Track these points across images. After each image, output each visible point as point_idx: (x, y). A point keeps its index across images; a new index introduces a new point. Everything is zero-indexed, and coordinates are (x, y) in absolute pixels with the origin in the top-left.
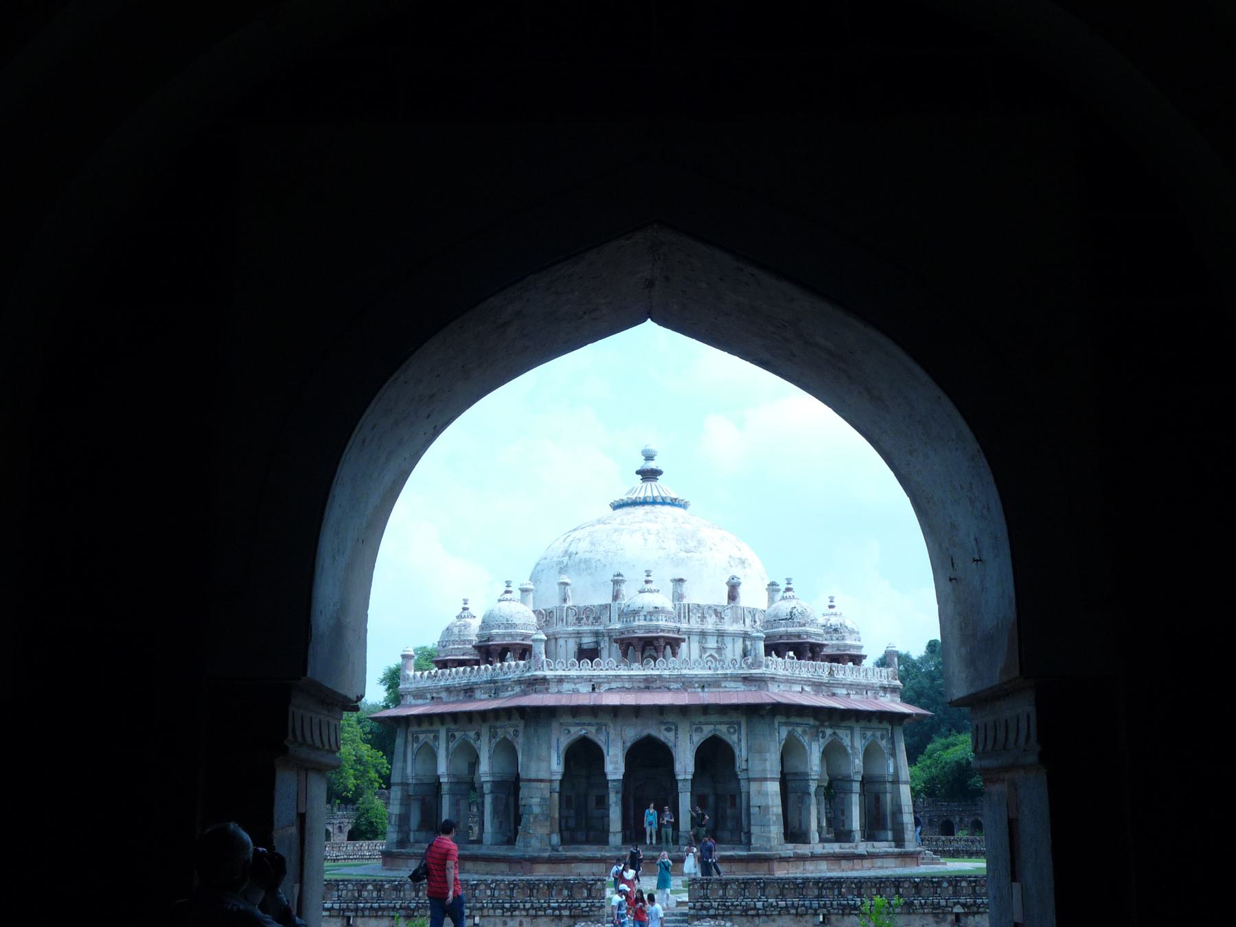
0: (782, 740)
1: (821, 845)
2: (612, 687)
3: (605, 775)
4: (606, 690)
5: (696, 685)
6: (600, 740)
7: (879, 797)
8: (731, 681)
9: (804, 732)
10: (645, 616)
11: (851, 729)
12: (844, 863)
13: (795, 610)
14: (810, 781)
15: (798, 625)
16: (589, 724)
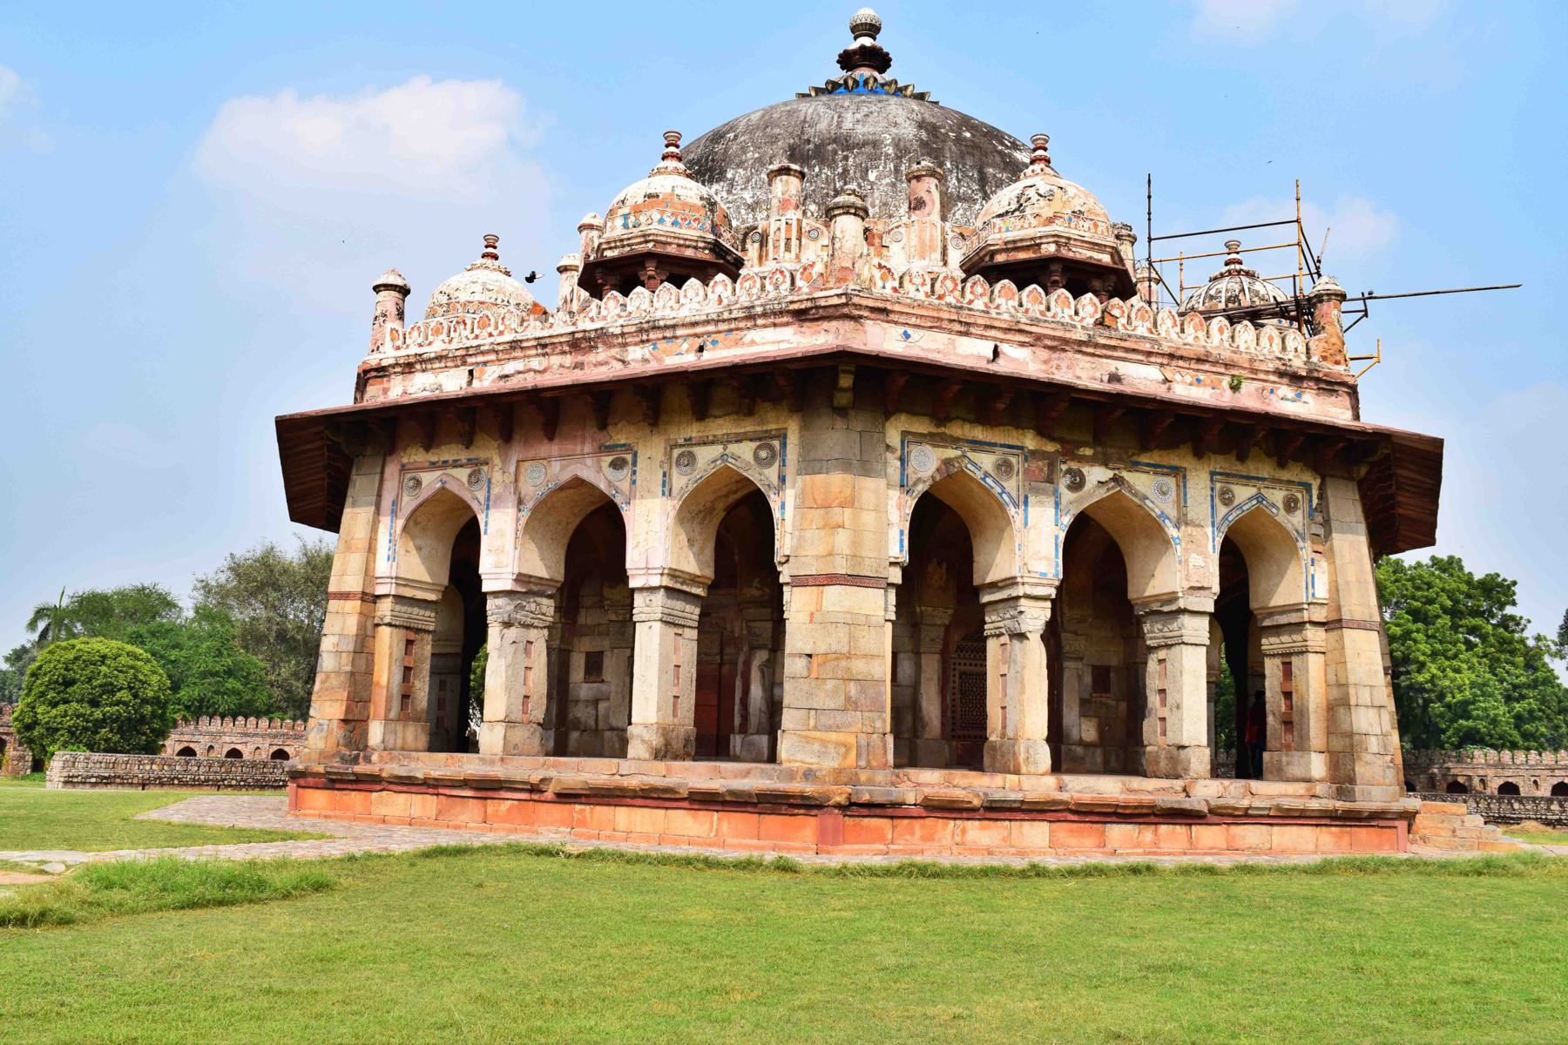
0: (919, 480)
1: (1051, 781)
2: (506, 372)
3: (478, 580)
4: (493, 381)
5: (685, 346)
6: (475, 498)
7: (1290, 663)
8: (765, 326)
9: (1005, 467)
10: (626, 217)
11: (1177, 472)
12: (1118, 833)
13: (1031, 193)
14: (1023, 601)
15: (1034, 222)
16: (456, 464)
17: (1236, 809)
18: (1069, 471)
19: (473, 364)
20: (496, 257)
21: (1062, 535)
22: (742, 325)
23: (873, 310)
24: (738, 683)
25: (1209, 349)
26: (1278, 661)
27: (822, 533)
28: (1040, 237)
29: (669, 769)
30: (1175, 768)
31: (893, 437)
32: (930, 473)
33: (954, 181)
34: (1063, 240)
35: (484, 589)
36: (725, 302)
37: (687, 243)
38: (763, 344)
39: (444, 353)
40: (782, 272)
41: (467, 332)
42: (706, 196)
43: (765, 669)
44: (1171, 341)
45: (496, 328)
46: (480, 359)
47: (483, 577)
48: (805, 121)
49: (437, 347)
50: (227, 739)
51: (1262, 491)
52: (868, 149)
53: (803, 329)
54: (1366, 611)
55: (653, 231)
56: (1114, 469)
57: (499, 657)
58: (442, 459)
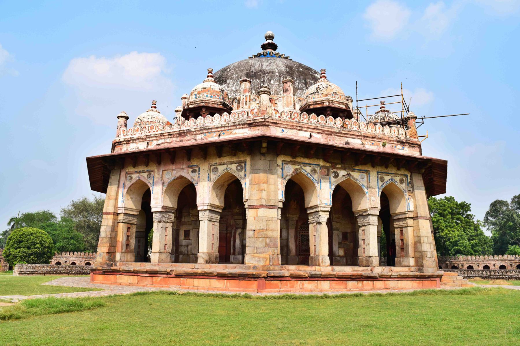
0: (287, 175)
1: (330, 268)
3: (150, 208)
4: (155, 146)
5: (215, 135)
6: (149, 182)
7: (403, 230)
8: (239, 128)
9: (314, 171)
10: (196, 95)
11: (367, 172)
12: (351, 284)
13: (321, 87)
14: (320, 212)
15: (322, 96)
16: (143, 172)
17: (387, 276)
18: (334, 172)
19: (148, 141)
20: (156, 108)
21: (332, 192)
22: (232, 128)
23: (273, 123)
24: (232, 239)
25: (376, 134)
26: (399, 230)
27: (258, 192)
28: (324, 100)
29: (210, 267)
30: (368, 263)
31: (279, 162)
32: (291, 173)
33: (297, 83)
34: (331, 101)
35: (152, 211)
36: (227, 121)
37: (215, 103)
38: (239, 134)
39: (139, 137)
40: (244, 112)
41: (147, 131)
42: (221, 88)
43: (240, 235)
44: (364, 132)
45: (156, 129)
46: (151, 139)
47: (152, 207)
48: (251, 65)
49: (137, 135)
50: (71, 259)
51: (393, 177)
52: (271, 74)
53: (251, 129)
54: (425, 214)
55: (204, 99)
56: (347, 171)
57: (157, 232)
58: (139, 170)
